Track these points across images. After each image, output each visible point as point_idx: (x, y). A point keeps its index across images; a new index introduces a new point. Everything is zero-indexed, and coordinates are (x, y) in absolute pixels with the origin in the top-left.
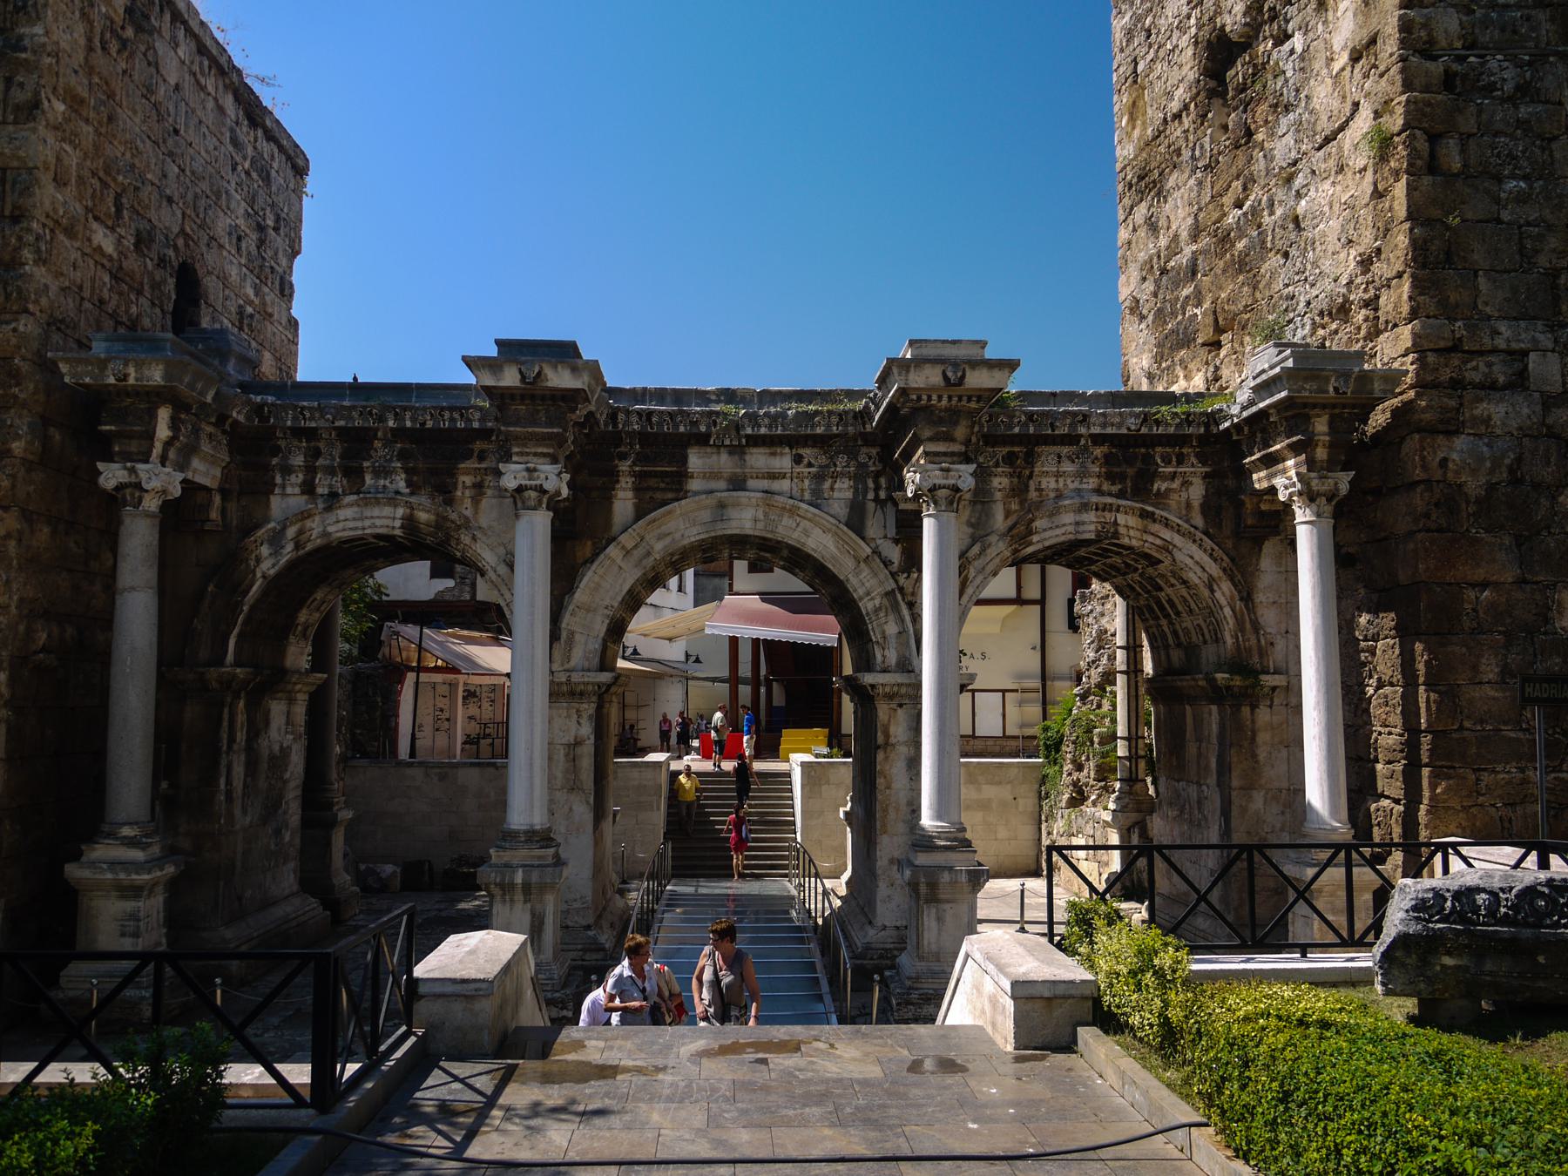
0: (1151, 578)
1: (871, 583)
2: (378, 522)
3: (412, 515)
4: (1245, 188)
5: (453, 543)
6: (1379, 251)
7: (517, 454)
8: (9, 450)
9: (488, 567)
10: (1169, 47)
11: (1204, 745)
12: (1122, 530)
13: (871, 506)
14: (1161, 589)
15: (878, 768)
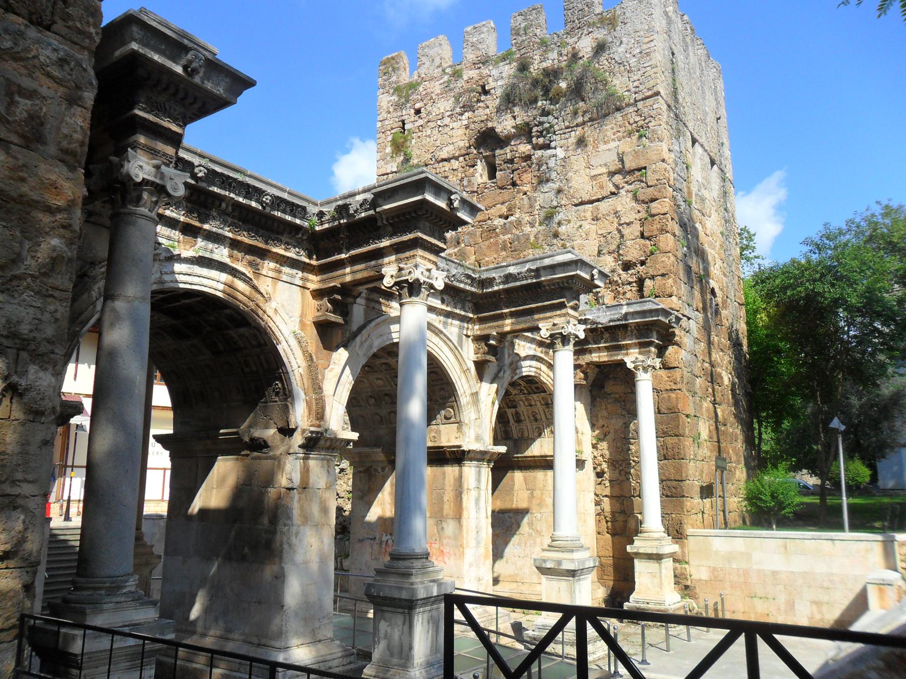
0: (514, 401)
1: (466, 386)
2: (205, 282)
3: (233, 281)
4: (509, 210)
5: (260, 313)
6: (643, 263)
7: (421, 256)
8: (80, 98)
9: (281, 338)
10: (439, 122)
11: (537, 493)
12: (542, 373)
13: (464, 337)
14: (515, 407)
15: (464, 505)
